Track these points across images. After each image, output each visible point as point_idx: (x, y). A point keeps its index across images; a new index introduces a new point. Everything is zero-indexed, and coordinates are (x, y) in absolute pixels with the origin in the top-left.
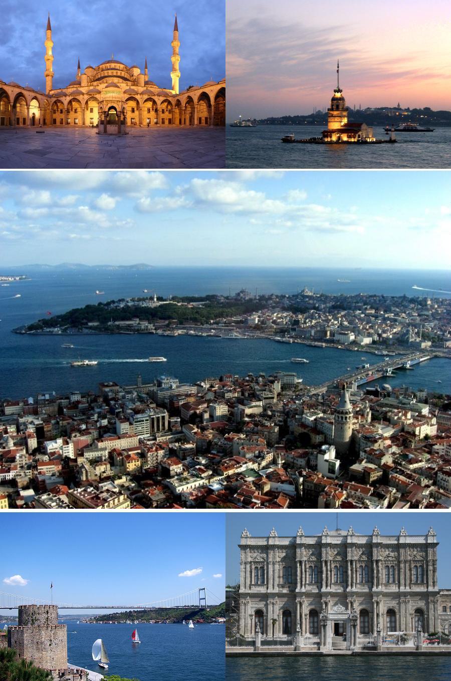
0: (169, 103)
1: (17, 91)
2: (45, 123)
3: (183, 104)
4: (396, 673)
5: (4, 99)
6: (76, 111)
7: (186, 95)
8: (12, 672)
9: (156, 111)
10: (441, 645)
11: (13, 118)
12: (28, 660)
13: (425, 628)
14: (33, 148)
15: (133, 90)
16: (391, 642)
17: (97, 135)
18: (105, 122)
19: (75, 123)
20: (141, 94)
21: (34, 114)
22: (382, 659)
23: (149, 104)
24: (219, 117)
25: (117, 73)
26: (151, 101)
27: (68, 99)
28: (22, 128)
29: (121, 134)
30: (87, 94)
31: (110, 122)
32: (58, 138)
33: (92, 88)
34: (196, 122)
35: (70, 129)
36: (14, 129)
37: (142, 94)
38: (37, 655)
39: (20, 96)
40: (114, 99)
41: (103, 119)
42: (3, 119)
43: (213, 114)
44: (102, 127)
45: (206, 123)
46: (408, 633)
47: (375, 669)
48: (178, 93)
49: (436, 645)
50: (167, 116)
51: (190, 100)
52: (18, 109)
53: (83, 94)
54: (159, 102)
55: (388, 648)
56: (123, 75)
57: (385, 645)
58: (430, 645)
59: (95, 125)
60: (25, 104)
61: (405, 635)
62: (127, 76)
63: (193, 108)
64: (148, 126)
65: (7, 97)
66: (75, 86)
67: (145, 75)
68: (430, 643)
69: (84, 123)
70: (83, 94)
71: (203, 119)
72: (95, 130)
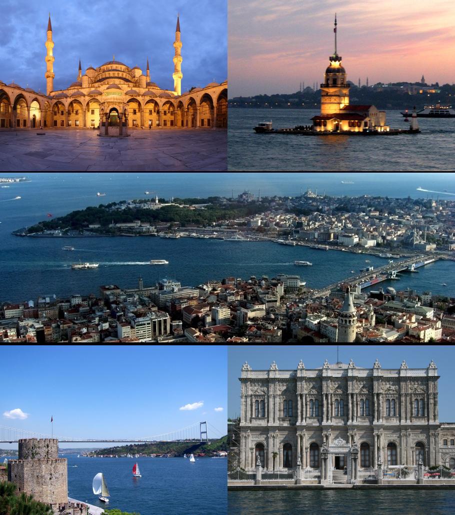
0: (172, 104)
1: (17, 92)
2: (45, 125)
3: (185, 105)
4: (397, 507)
5: (5, 100)
6: (77, 113)
7: (189, 96)
8: (12, 506)
9: (158, 112)
10: (442, 479)
11: (13, 120)
12: (28, 494)
13: (426, 462)
14: (33, 150)
15: (135, 91)
16: (391, 476)
17: (98, 137)
18: (106, 124)
19: (76, 125)
20: (142, 96)
21: (34, 115)
22: (383, 492)
23: (151, 106)
24: (222, 119)
25: (118, 74)
26: (153, 103)
27: (70, 100)
28: (22, 130)
29: (123, 135)
30: (89, 95)
31: (111, 124)
32: (59, 140)
33: (93, 89)
34: (198, 124)
35: (71, 131)
36: (15, 131)
37: (144, 95)
38: (37, 489)
39: (20, 97)
40: (116, 101)
41: (105, 121)
42: (3, 121)
43: (215, 116)
44: (103, 129)
45: (209, 124)
46: (409, 466)
47: (377, 503)
48: (180, 95)
49: (437, 478)
50: (169, 117)
51: (192, 102)
52: (18, 111)
53: (84, 95)
54: (161, 104)
55: (389, 482)
56: (124, 76)
57: (386, 479)
58: (431, 479)
59: (96, 127)
60: (26, 105)
61: (406, 468)
62: (129, 77)
63: (195, 110)
64: (150, 127)
65: (8, 98)
66: (76, 87)
67: (147, 76)
68: (431, 476)
69: (85, 125)
70: (84, 95)
71: (206, 121)
72: (97, 132)
